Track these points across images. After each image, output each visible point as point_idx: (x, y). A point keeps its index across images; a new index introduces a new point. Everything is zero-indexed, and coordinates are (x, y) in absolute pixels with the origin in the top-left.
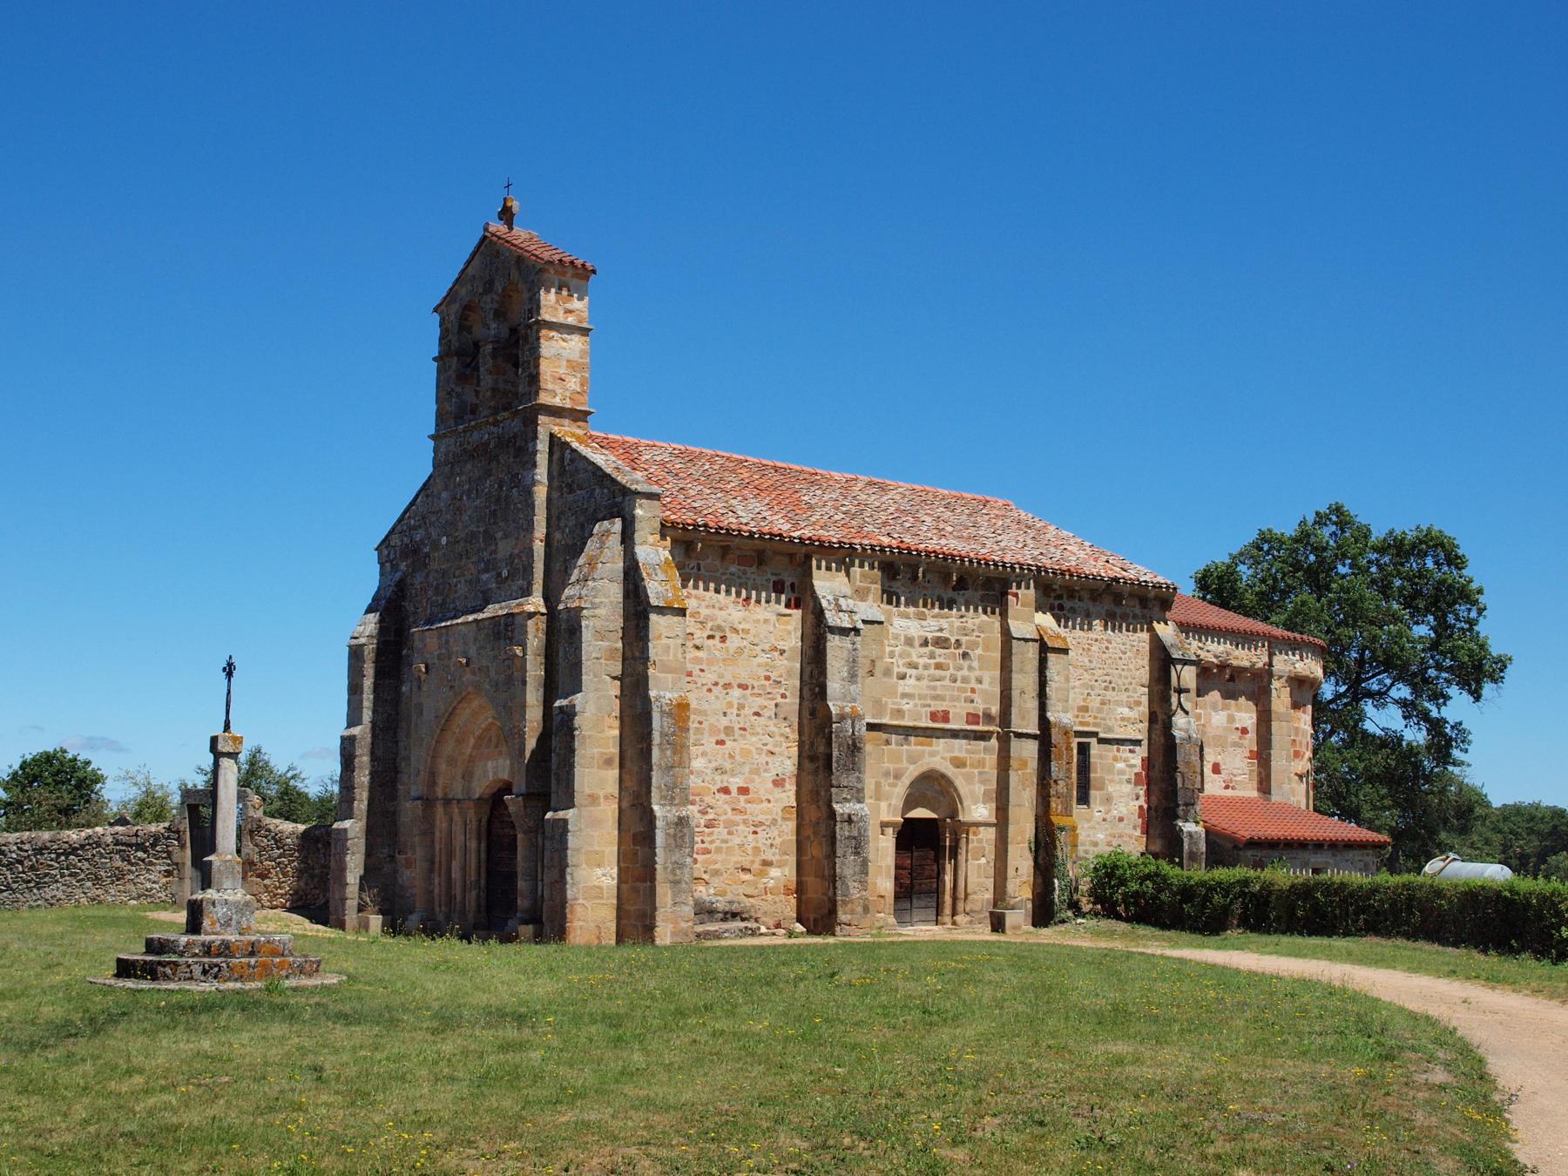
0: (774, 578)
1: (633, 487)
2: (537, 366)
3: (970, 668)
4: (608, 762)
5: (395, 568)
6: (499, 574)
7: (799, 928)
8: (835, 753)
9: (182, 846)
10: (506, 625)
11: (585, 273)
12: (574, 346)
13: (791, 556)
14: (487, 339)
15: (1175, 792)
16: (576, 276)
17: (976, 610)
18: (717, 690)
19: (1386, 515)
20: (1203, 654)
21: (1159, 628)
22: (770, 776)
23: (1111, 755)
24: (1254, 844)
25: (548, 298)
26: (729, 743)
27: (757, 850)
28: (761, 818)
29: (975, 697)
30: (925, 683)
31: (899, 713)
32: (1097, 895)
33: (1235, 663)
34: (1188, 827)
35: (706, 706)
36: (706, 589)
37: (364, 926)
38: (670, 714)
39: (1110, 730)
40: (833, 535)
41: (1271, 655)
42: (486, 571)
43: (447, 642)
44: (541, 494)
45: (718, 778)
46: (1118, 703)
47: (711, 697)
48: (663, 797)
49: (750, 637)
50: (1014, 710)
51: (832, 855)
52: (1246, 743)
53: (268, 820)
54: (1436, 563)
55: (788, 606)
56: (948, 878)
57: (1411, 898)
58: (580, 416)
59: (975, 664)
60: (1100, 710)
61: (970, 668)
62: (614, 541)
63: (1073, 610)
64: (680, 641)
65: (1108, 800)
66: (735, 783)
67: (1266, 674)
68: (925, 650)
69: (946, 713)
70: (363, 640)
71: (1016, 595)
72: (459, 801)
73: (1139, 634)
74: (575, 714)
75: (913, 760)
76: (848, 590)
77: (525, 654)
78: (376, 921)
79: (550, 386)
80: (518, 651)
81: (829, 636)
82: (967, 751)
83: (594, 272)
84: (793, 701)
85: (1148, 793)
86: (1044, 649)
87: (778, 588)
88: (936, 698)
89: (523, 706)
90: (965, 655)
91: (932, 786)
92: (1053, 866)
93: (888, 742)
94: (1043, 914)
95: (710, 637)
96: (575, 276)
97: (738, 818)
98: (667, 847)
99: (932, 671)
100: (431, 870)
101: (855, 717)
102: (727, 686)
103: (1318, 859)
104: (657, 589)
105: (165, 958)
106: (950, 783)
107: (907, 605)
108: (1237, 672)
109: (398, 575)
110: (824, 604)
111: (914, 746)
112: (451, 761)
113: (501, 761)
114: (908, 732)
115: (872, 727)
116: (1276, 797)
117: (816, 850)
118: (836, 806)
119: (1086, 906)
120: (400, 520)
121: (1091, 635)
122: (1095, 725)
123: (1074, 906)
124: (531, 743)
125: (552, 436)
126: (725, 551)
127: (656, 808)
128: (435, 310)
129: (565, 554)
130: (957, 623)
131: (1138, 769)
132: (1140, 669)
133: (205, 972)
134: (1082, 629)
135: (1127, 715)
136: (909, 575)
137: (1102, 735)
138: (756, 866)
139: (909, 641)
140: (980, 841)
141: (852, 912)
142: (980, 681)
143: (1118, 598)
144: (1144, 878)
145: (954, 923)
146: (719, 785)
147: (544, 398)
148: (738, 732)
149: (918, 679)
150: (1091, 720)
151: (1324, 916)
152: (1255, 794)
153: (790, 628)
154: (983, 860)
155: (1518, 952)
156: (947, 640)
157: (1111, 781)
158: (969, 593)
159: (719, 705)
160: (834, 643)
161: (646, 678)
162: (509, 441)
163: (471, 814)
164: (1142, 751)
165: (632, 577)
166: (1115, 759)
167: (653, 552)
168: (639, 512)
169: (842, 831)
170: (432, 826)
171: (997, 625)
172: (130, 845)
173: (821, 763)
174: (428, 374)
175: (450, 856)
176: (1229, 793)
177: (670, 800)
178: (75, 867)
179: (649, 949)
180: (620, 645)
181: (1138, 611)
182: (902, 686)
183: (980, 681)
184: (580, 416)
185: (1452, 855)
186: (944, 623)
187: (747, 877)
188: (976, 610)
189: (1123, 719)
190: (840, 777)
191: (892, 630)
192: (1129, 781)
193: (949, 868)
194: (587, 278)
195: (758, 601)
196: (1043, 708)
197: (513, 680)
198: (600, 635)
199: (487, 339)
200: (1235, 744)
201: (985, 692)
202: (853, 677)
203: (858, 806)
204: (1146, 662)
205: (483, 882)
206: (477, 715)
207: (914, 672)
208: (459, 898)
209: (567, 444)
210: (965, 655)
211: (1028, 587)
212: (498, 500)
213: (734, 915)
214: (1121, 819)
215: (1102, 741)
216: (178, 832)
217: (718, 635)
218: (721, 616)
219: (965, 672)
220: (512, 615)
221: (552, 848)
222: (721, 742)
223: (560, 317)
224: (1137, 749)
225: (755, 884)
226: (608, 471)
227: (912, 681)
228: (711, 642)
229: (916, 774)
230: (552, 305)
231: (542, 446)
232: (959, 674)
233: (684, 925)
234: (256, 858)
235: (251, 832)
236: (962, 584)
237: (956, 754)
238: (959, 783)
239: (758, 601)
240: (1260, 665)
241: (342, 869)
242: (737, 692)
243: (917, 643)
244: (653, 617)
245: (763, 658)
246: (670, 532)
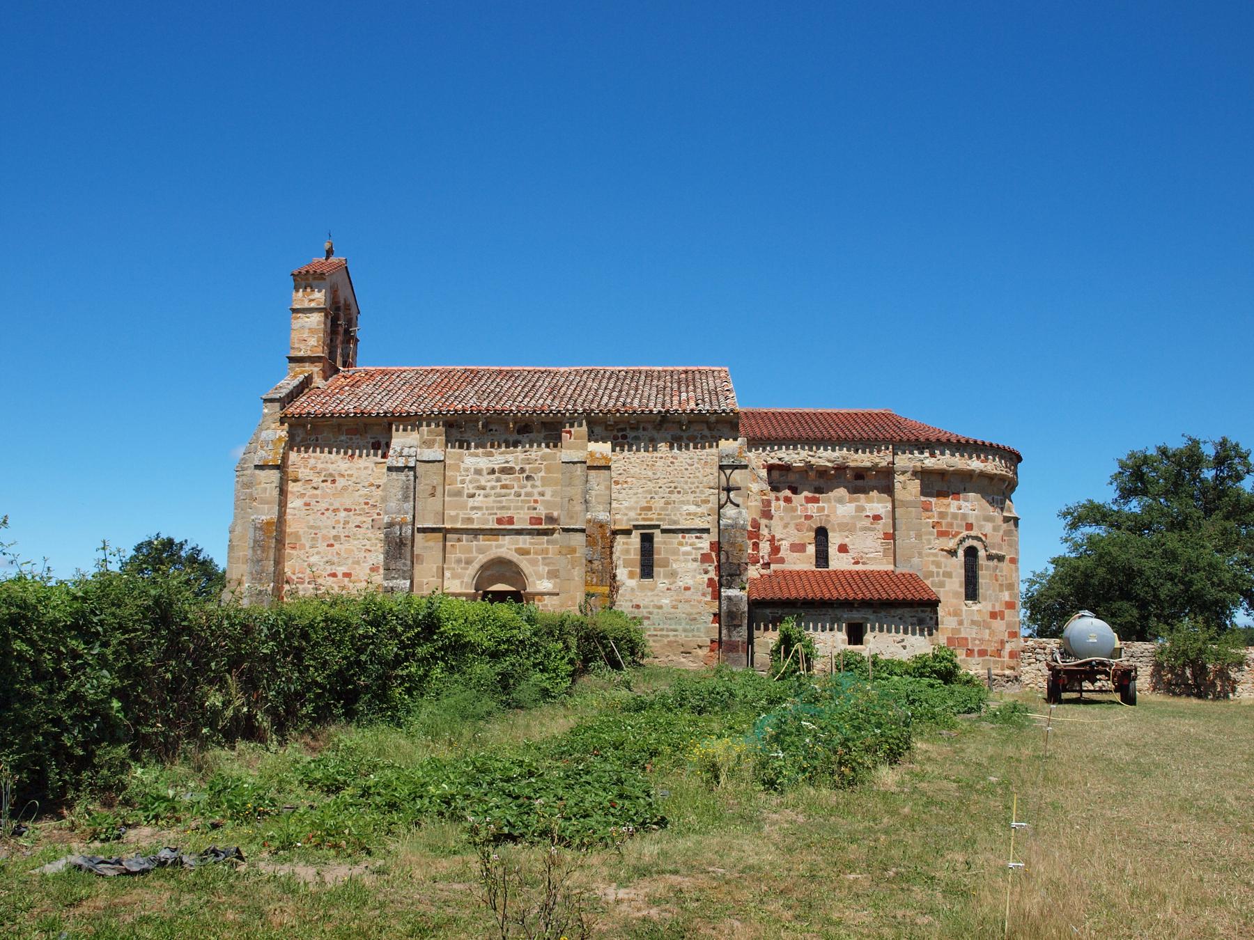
3: (533, 486)
16: (315, 279)
17: (539, 445)
18: (327, 514)
20: (813, 461)
22: (367, 566)
23: (676, 541)
26: (337, 546)
29: (538, 506)
30: (492, 498)
31: (470, 520)
33: (852, 464)
35: (320, 524)
38: (261, 529)
39: (675, 522)
41: (895, 454)
45: (328, 568)
46: (683, 502)
47: (324, 518)
49: (354, 479)
59: (538, 483)
60: (662, 509)
63: (637, 438)
65: (673, 574)
66: (340, 570)
68: (493, 476)
71: (570, 432)
73: (708, 450)
75: (481, 551)
82: (531, 543)
88: (502, 508)
90: (528, 478)
91: (501, 568)
93: (459, 540)
102: (334, 510)
106: (517, 566)
107: (476, 447)
108: (860, 474)
111: (482, 541)
114: (476, 533)
121: (655, 454)
122: (658, 520)
130: (522, 456)
134: (646, 450)
136: (462, 429)
139: (478, 472)
150: (655, 516)
156: (512, 468)
157: (675, 561)
159: (330, 523)
166: (681, 544)
176: (859, 567)
181: (706, 432)
186: (510, 457)
188: (539, 445)
189: (689, 514)
191: (462, 465)
192: (695, 560)
195: (360, 456)
200: (865, 529)
207: (482, 492)
211: (580, 425)
214: (687, 589)
215: (664, 531)
217: (330, 479)
218: (332, 468)
219: (529, 489)
222: (332, 545)
223: (306, 305)
224: (705, 535)
227: (481, 498)
229: (485, 560)
232: (523, 491)
237: (521, 546)
238: (524, 564)
239: (360, 456)
240: (884, 464)
242: (343, 514)
243: (485, 472)
245: (364, 491)
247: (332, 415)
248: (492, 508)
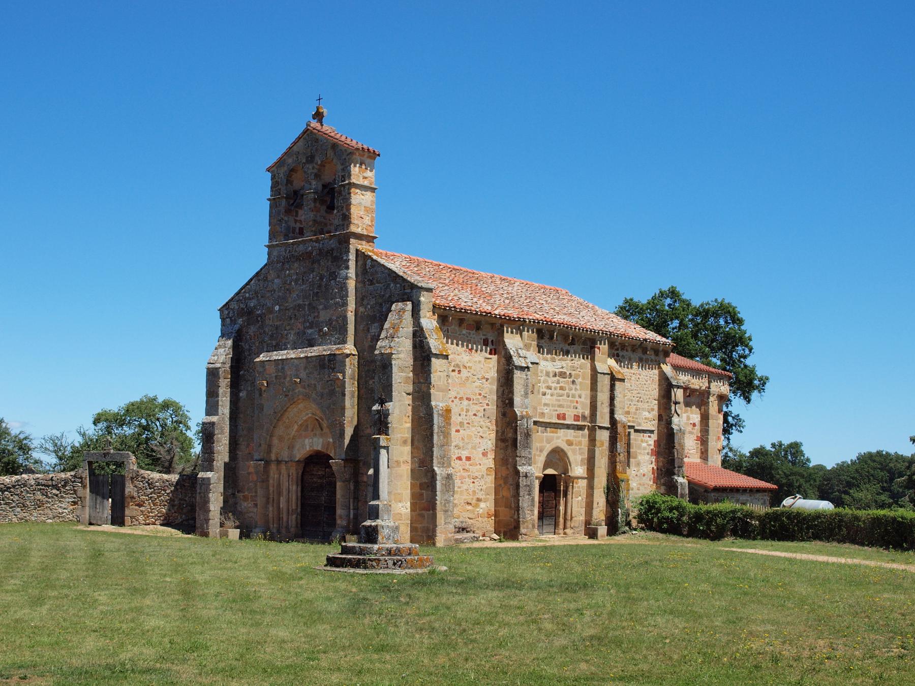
0: (484, 337)
1: (419, 285)
2: (349, 209)
4: (405, 442)
5: (233, 322)
6: (321, 330)
7: (496, 536)
8: (519, 438)
9: (84, 487)
10: (329, 361)
11: (374, 155)
12: (368, 197)
13: (493, 325)
14: (311, 190)
15: (673, 460)
16: (370, 157)
19: (699, 294)
21: (663, 366)
22: (481, 450)
24: (717, 489)
25: (355, 170)
27: (474, 492)
28: (477, 474)
29: (579, 406)
30: (555, 397)
31: (543, 414)
32: (641, 518)
33: (692, 386)
34: (680, 480)
36: (452, 344)
37: (224, 534)
38: (442, 415)
39: (639, 425)
40: (514, 313)
41: (709, 382)
42: (311, 327)
43: (283, 368)
44: (351, 284)
46: (643, 409)
48: (439, 463)
49: (472, 371)
50: (598, 413)
51: (517, 495)
52: (695, 431)
53: (142, 471)
54: (726, 322)
55: (491, 354)
56: (562, 508)
57: (841, 521)
58: (370, 239)
59: (578, 387)
60: (635, 414)
61: (576, 389)
62: (408, 316)
64: (446, 374)
66: (464, 454)
67: (706, 394)
69: (564, 414)
70: (218, 365)
71: (599, 348)
72: (286, 462)
74: (389, 415)
76: (521, 345)
77: (344, 378)
78: (234, 533)
79: (356, 222)
80: (340, 376)
81: (515, 371)
83: (379, 155)
84: (492, 409)
85: (657, 461)
86: (613, 379)
87: (486, 343)
88: (560, 406)
89: (343, 408)
92: (618, 501)
94: (613, 529)
95: (453, 371)
96: (369, 156)
97: (465, 474)
98: (442, 491)
99: (558, 391)
100: (268, 502)
101: (528, 417)
102: (461, 399)
103: (743, 498)
104: (435, 342)
105: (367, 557)
109: (237, 327)
110: (512, 353)
112: (281, 439)
113: (315, 439)
115: (535, 423)
116: (710, 463)
117: (506, 493)
118: (519, 468)
119: (634, 523)
120: (237, 294)
121: (632, 371)
122: (633, 422)
123: (628, 524)
124: (349, 432)
125: (357, 250)
126: (461, 321)
127: (436, 468)
128: (268, 170)
129: (374, 319)
130: (570, 363)
131: (652, 447)
132: (653, 391)
133: (394, 564)
135: (648, 417)
137: (636, 428)
138: (474, 502)
139: (548, 374)
140: (579, 487)
141: (527, 528)
142: (580, 397)
143: (645, 350)
144: (671, 509)
145: (565, 533)
146: (457, 456)
147: (353, 229)
148: (466, 425)
149: (552, 395)
151: (787, 530)
152: (699, 460)
153: (491, 366)
154: (580, 498)
155: (907, 549)
156: (565, 373)
158: (575, 347)
160: (518, 375)
161: (430, 394)
162: (328, 252)
163: (293, 471)
164: (654, 437)
165: (419, 337)
166: (642, 441)
167: (429, 322)
168: (422, 299)
169: (523, 482)
170: (268, 476)
171: (589, 365)
172: (48, 486)
173: (510, 442)
174: (265, 208)
175: (279, 494)
177: (442, 465)
178: (8, 499)
179: (432, 549)
180: (411, 374)
181: (653, 357)
182: (545, 399)
183: (580, 397)
184: (370, 239)
185: (798, 496)
186: (564, 363)
187: (470, 507)
190: (521, 451)
193: (562, 502)
194: (374, 159)
196: (612, 412)
197: (335, 393)
198: (401, 369)
199: (311, 190)
200: (690, 433)
201: (582, 403)
202: (526, 395)
203: (529, 468)
204: (657, 386)
205: (299, 510)
206: (303, 411)
208: (285, 519)
209: (370, 257)
210: (573, 382)
212: (320, 286)
213: (463, 529)
215: (637, 431)
216: (81, 478)
217: (457, 369)
219: (573, 392)
220: (335, 355)
221: (365, 488)
225: (473, 512)
226: (401, 274)
228: (453, 374)
230: (357, 174)
231: (352, 257)
232: (571, 393)
233: (450, 535)
234: (135, 494)
235: (132, 478)
236: (572, 343)
238: (570, 454)
239: (476, 351)
240: (704, 388)
241: (206, 501)
242: (465, 402)
244: (433, 360)
245: (478, 383)
246: (436, 310)
247: (477, 314)
248: (553, 406)
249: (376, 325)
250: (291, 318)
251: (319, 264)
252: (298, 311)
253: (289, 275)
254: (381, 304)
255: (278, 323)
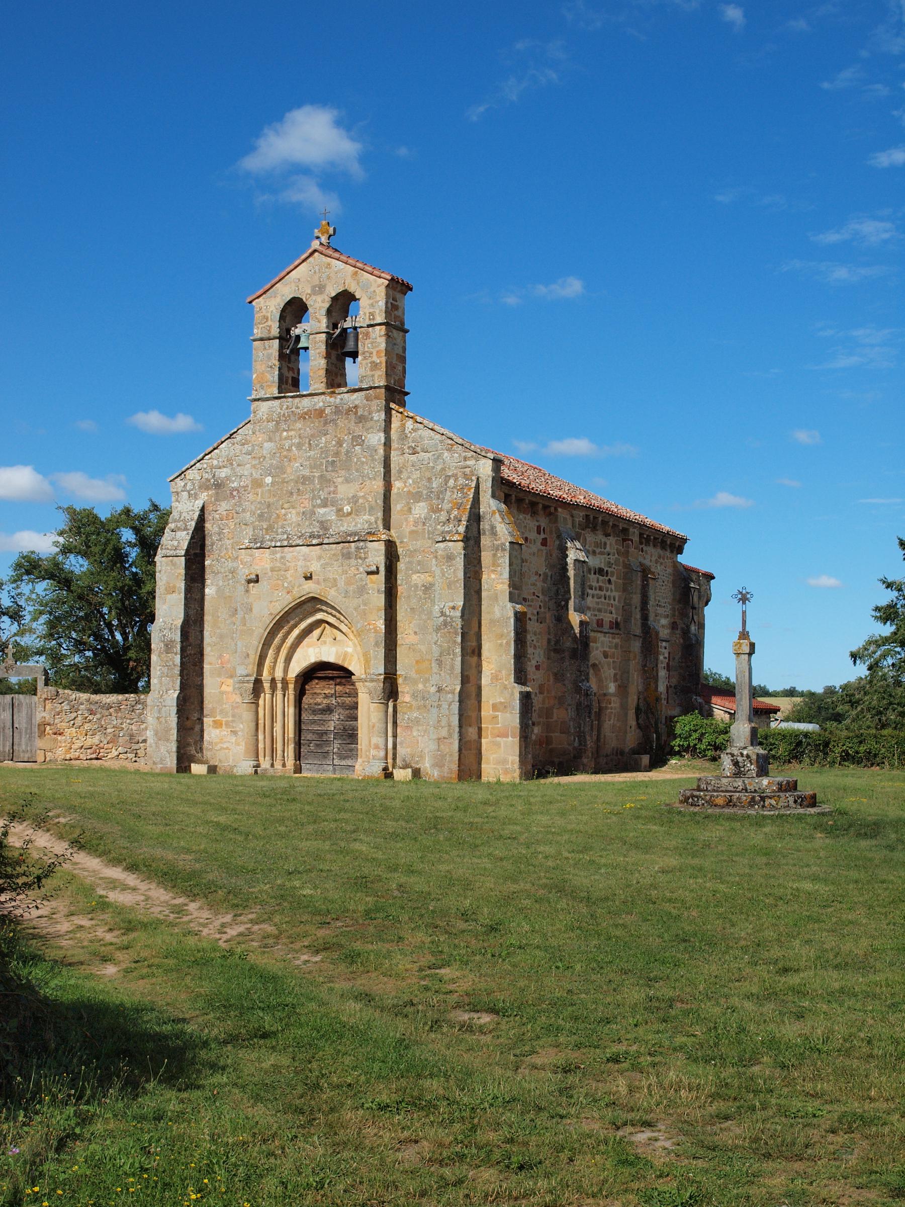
0: (537, 524)
13: (545, 507)
42: (325, 505)
61: (611, 590)
88: (600, 610)
133: (795, 802)
162: (349, 410)
212: (337, 454)
249: (422, 504)
250: (292, 493)
251: (336, 424)
252: (303, 483)
253: (286, 439)
254: (429, 479)
255: (271, 500)
